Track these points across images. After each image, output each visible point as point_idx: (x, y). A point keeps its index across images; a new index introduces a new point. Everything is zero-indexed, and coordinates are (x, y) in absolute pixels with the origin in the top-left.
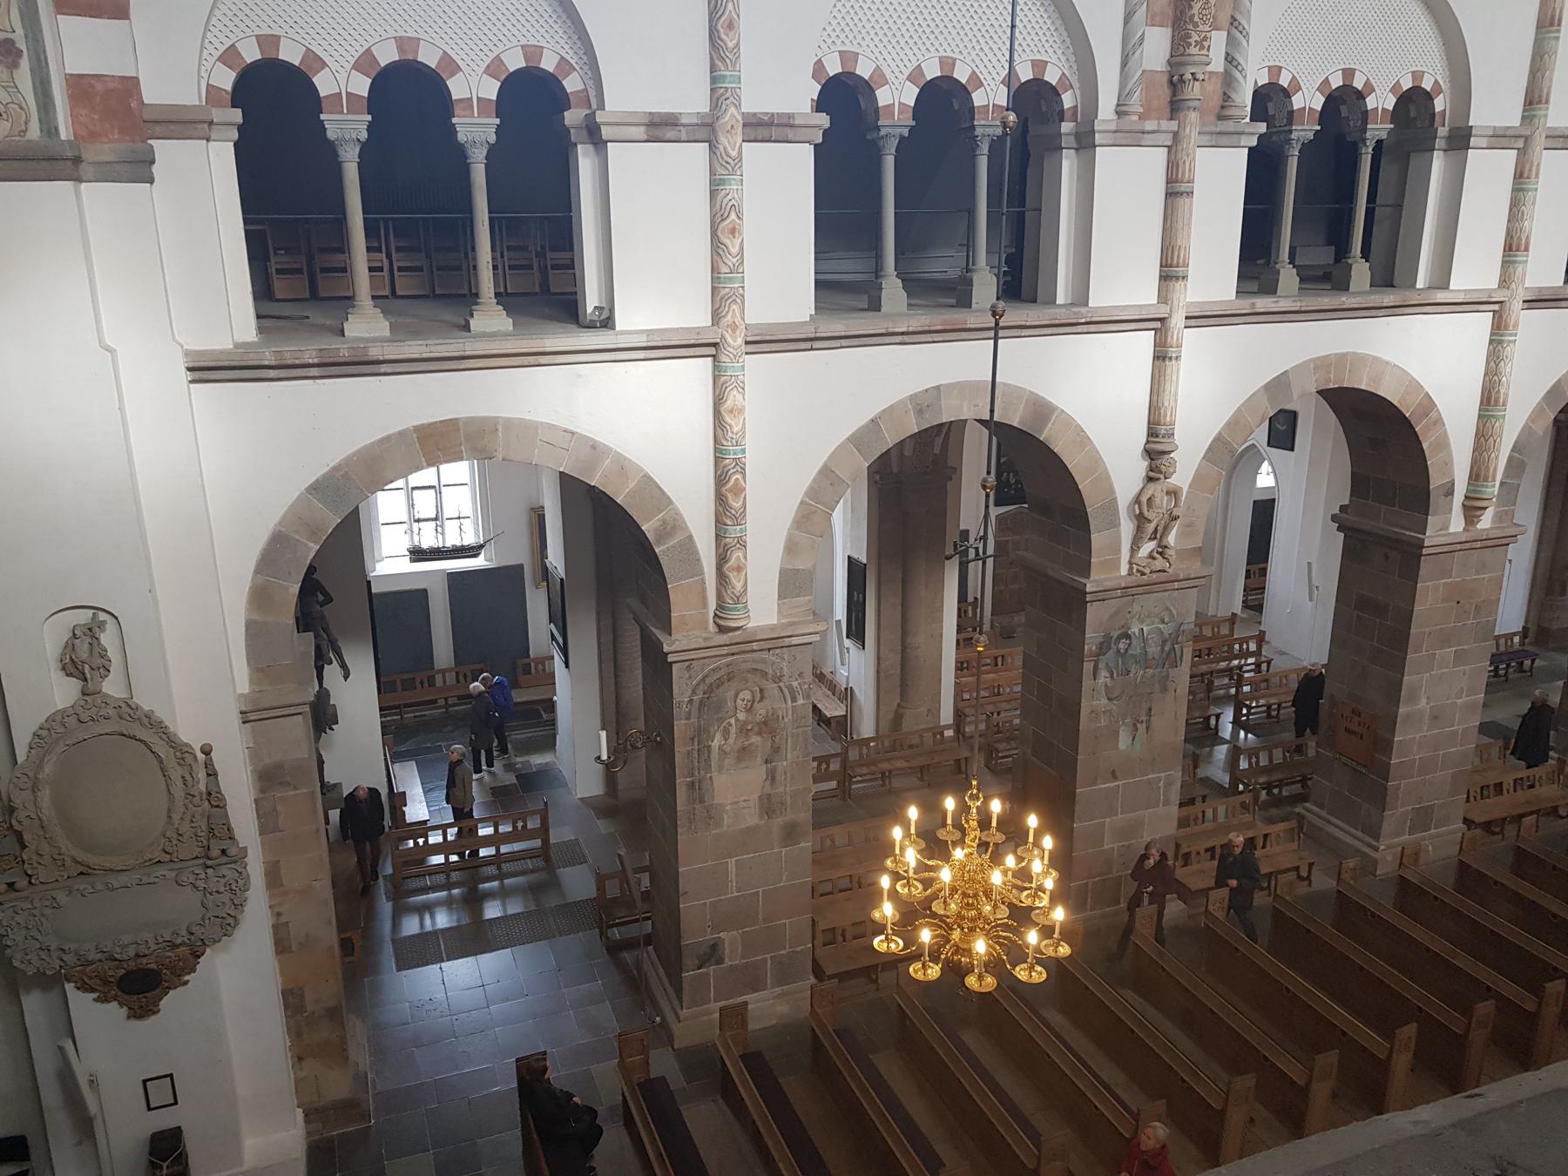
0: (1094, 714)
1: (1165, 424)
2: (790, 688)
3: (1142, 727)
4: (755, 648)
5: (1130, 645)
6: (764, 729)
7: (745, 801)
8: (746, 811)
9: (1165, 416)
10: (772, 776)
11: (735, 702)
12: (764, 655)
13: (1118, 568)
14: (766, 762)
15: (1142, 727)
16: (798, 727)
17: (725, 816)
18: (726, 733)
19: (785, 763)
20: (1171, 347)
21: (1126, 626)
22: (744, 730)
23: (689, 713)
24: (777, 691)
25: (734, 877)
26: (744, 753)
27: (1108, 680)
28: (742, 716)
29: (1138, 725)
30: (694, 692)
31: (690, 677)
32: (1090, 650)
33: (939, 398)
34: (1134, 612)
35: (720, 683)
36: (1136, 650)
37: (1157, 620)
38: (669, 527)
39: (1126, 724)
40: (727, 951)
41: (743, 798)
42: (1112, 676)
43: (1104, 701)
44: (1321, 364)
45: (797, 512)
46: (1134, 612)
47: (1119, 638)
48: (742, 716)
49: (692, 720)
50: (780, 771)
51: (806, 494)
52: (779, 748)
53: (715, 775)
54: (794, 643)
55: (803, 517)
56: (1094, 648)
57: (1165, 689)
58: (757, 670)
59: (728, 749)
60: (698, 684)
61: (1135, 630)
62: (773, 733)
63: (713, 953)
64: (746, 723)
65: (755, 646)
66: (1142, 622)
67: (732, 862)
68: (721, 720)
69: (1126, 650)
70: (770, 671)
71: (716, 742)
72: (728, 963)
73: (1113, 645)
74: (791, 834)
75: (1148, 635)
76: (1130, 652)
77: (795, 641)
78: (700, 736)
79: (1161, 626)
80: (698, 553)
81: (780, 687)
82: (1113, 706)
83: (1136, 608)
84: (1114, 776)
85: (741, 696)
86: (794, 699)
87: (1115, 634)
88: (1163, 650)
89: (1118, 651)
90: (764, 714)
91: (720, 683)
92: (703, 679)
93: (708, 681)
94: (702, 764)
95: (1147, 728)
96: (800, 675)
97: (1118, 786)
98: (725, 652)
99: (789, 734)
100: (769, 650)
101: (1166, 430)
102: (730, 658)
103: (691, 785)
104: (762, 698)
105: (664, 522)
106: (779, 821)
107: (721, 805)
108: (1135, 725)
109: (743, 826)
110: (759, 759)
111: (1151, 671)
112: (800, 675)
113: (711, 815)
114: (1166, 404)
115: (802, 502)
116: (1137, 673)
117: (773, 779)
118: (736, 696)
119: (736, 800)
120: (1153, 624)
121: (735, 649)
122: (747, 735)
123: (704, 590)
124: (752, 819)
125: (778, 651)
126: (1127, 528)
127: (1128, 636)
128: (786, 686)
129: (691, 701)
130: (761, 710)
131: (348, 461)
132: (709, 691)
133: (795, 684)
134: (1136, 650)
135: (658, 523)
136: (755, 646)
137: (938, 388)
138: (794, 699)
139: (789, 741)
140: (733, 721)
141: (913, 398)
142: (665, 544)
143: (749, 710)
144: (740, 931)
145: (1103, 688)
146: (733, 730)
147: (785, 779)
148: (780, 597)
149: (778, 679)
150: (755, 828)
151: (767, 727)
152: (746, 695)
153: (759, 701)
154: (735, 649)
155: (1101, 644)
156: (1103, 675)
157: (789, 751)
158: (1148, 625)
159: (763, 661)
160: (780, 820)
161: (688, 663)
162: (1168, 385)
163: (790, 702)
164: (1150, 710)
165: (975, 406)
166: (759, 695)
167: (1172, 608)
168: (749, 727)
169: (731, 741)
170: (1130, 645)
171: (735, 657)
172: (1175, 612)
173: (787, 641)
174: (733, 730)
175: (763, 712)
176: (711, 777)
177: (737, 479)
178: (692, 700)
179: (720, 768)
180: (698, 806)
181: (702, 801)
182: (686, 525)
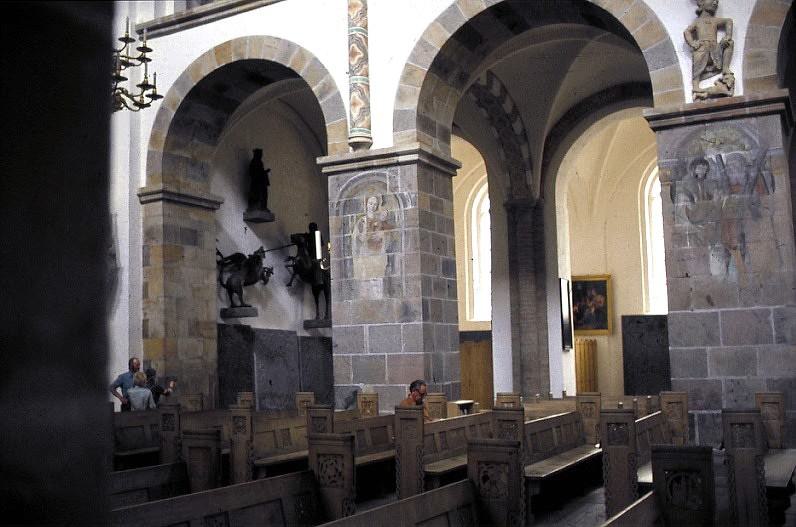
2: (402, 195)
4: (375, 164)
5: (708, 170)
10: (391, 260)
13: (682, 97)
16: (409, 226)
21: (702, 153)
22: (372, 227)
23: (338, 211)
24: (393, 199)
27: (689, 204)
28: (371, 215)
29: (732, 252)
30: (341, 197)
36: (716, 174)
39: (717, 249)
42: (692, 199)
43: (687, 224)
47: (694, 164)
50: (397, 259)
51: (410, 58)
56: (669, 173)
57: (757, 216)
61: (711, 156)
65: (375, 162)
66: (719, 149)
67: (366, 326)
69: (705, 176)
71: (354, 234)
76: (708, 177)
78: (344, 226)
79: (742, 153)
84: (710, 302)
85: (370, 200)
86: (405, 205)
87: (691, 160)
88: (748, 176)
95: (743, 256)
97: (716, 313)
103: (340, 263)
105: (325, 84)
106: (396, 302)
108: (726, 251)
111: (737, 197)
115: (407, 65)
116: (721, 198)
120: (732, 150)
126: (685, 65)
127: (705, 163)
129: (339, 203)
130: (383, 213)
131: (188, 69)
133: (405, 193)
134: (716, 174)
136: (375, 162)
140: (365, 219)
145: (684, 211)
146: (365, 226)
150: (380, 304)
151: (387, 224)
158: (725, 152)
163: (402, 207)
164: (743, 236)
168: (376, 224)
169: (365, 232)
170: (708, 170)
173: (395, 159)
174: (365, 226)
179: (358, 252)
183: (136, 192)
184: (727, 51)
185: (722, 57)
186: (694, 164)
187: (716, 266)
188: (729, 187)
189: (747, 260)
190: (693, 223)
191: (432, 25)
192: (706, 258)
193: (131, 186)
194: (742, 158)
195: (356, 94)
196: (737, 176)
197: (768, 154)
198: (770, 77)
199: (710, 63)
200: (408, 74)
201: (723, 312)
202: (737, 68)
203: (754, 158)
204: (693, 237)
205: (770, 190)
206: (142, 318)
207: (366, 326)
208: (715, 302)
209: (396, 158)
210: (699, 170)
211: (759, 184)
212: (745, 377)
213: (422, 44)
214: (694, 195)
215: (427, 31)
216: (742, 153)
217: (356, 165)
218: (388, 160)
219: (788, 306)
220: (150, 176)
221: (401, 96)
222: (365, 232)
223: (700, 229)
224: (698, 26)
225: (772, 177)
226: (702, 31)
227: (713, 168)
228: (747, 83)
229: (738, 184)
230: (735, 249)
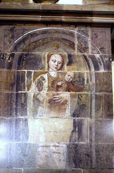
2: (93, 58)
6: (72, 87)
7: (55, 146)
10: (78, 126)
18: (40, 86)
22: (54, 86)
24: (82, 59)
30: (15, 49)
60: (19, 43)
70: (76, 42)
81: (85, 57)
85: (53, 58)
86: (97, 68)
117: (80, 132)
118: (49, 57)
119: (48, 144)
121: (48, 18)
129: (12, 55)
130: (70, 73)
133: (97, 56)
138: (97, 68)
140: (46, 76)
146: (46, 84)
154: (48, 18)
168: (59, 84)
169: (44, 92)
173: (89, 19)
174: (46, 84)
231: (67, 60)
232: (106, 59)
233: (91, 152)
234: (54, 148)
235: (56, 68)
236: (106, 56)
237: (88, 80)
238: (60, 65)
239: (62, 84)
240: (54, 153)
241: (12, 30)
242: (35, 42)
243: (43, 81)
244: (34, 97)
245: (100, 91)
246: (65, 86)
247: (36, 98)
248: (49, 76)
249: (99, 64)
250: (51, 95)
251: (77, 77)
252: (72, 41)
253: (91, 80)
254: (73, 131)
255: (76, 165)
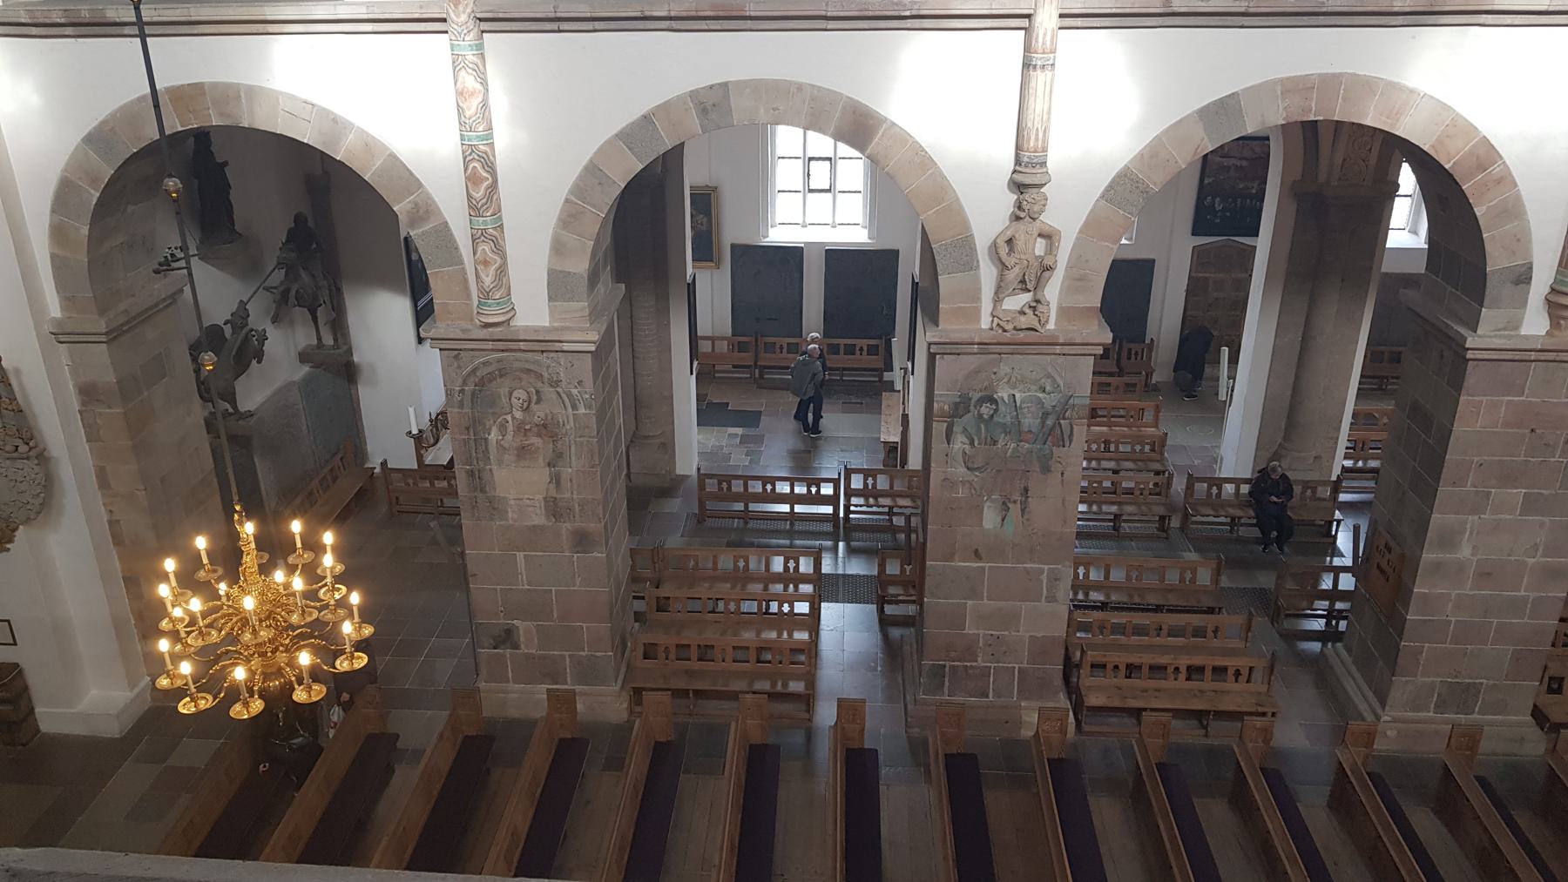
0: (948, 482)
1: (1028, 151)
2: (569, 395)
3: (1015, 509)
4: (523, 348)
6: (544, 432)
7: (529, 499)
8: (531, 509)
9: (1029, 139)
10: (556, 480)
11: (510, 399)
12: (538, 357)
13: (978, 318)
14: (549, 465)
15: (1015, 509)
17: (509, 510)
18: (503, 429)
19: (570, 470)
20: (1036, 52)
22: (521, 429)
24: (554, 396)
25: (523, 570)
26: (523, 452)
27: (967, 447)
29: (1010, 505)
30: (464, 383)
31: (459, 367)
32: (942, 409)
33: (726, 96)
34: (1002, 373)
35: (491, 378)
36: (1005, 416)
37: (1033, 387)
38: (421, 211)
40: (522, 639)
41: (527, 496)
42: (972, 443)
43: (963, 470)
44: (1293, 87)
45: (561, 210)
46: (1002, 373)
47: (981, 401)
48: (518, 415)
49: (466, 410)
51: (571, 192)
52: (562, 453)
53: (494, 467)
54: (565, 348)
55: (569, 216)
56: (946, 407)
57: (1046, 470)
58: (531, 370)
59: (506, 445)
60: (469, 375)
61: (1003, 394)
62: (554, 437)
63: (507, 638)
64: (523, 422)
65: (522, 345)
66: (1014, 387)
67: (520, 555)
68: (496, 415)
70: (545, 375)
71: (494, 436)
72: (524, 650)
73: (972, 408)
74: (582, 541)
75: (1022, 402)
76: (995, 419)
77: (566, 347)
79: (1041, 395)
80: (455, 242)
81: (558, 393)
82: (974, 477)
83: (1004, 369)
84: (977, 555)
85: (515, 394)
86: (574, 407)
87: (976, 396)
88: (1043, 423)
89: (980, 416)
90: (543, 415)
91: (491, 378)
92: (474, 371)
93: (478, 374)
94: (481, 455)
95: (1023, 511)
96: (580, 383)
97: (983, 568)
98: (491, 347)
99: (572, 442)
100: (542, 351)
101: (1029, 157)
102: (501, 355)
104: (539, 401)
106: (566, 527)
107: (504, 498)
109: (529, 524)
110: (541, 461)
111: (1027, 446)
112: (580, 383)
113: (495, 507)
114: (1030, 124)
115: (567, 201)
117: (558, 484)
118: (511, 394)
119: (521, 497)
121: (500, 345)
122: (525, 435)
123: (466, 280)
124: (538, 518)
125: (553, 355)
126: (987, 274)
127: (993, 401)
128: (565, 392)
129: (462, 391)
130: (539, 412)
132: (481, 383)
133: (575, 391)
135: (410, 206)
136: (522, 345)
137: (725, 85)
138: (574, 407)
139: (573, 449)
140: (509, 418)
141: (694, 94)
142: (420, 228)
143: (526, 410)
144: (535, 623)
146: (510, 427)
147: (571, 486)
148: (550, 299)
149: (555, 383)
152: (520, 394)
153: (536, 403)
154: (500, 345)
155: (956, 405)
156: (959, 442)
157: (573, 458)
159: (537, 363)
160: (568, 525)
161: (456, 352)
162: (1032, 99)
163: (570, 410)
164: (1026, 490)
165: (774, 109)
166: (535, 397)
167: (1056, 376)
168: (527, 427)
169: (509, 437)
170: (996, 411)
171: (506, 354)
172: (1059, 380)
173: (558, 346)
174: (510, 427)
175: (542, 415)
176: (491, 470)
177: (475, 167)
178: (463, 390)
179: (500, 462)
180: (479, 495)
181: (483, 491)
182: (440, 211)
183: (48, 328)
184: (1047, 274)
185: (1039, 279)
186: (981, 401)
187: (990, 518)
188: (1016, 431)
189: (1026, 517)
190: (968, 469)
191: (608, 142)
192: (979, 511)
193: (37, 326)
194: (1040, 402)
195: (486, 248)
196: (1030, 421)
197: (1071, 401)
198: (1090, 309)
199: (1023, 282)
200: (570, 218)
201: (990, 567)
202: (1053, 291)
203: (1054, 404)
204: (967, 485)
205: (1067, 444)
206: (105, 517)
207: (520, 555)
208: (983, 555)
209: (561, 344)
210: (986, 410)
211: (1054, 432)
212: (1006, 633)
213: (593, 171)
214: (976, 438)
215: (601, 151)
216: (1041, 395)
217: (490, 345)
218: (543, 344)
219: (1064, 566)
220: (68, 300)
221: (558, 248)
222: (509, 437)
223: (977, 476)
224: (1017, 236)
225: (1072, 428)
226: (1020, 244)
227: (1002, 408)
228: (1064, 312)
229: (1030, 431)
230: (1015, 502)
231: (535, 398)
232: (587, 396)
233: (573, 506)
234: (528, 501)
235: (521, 408)
236: (586, 393)
237: (564, 422)
238: (526, 404)
239: (531, 427)
240: (528, 506)
241: (456, 357)
242: (489, 373)
243: (507, 424)
244: (497, 442)
245: (580, 437)
246: (535, 430)
247: (501, 448)
248: (513, 418)
249: (577, 402)
250: (518, 440)
251: (549, 418)
252: (539, 372)
253: (568, 422)
254: (550, 482)
255: (556, 519)
